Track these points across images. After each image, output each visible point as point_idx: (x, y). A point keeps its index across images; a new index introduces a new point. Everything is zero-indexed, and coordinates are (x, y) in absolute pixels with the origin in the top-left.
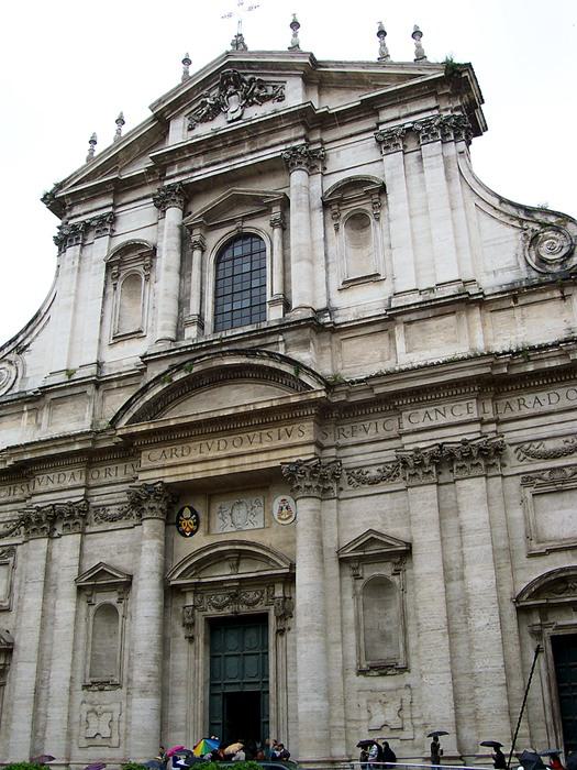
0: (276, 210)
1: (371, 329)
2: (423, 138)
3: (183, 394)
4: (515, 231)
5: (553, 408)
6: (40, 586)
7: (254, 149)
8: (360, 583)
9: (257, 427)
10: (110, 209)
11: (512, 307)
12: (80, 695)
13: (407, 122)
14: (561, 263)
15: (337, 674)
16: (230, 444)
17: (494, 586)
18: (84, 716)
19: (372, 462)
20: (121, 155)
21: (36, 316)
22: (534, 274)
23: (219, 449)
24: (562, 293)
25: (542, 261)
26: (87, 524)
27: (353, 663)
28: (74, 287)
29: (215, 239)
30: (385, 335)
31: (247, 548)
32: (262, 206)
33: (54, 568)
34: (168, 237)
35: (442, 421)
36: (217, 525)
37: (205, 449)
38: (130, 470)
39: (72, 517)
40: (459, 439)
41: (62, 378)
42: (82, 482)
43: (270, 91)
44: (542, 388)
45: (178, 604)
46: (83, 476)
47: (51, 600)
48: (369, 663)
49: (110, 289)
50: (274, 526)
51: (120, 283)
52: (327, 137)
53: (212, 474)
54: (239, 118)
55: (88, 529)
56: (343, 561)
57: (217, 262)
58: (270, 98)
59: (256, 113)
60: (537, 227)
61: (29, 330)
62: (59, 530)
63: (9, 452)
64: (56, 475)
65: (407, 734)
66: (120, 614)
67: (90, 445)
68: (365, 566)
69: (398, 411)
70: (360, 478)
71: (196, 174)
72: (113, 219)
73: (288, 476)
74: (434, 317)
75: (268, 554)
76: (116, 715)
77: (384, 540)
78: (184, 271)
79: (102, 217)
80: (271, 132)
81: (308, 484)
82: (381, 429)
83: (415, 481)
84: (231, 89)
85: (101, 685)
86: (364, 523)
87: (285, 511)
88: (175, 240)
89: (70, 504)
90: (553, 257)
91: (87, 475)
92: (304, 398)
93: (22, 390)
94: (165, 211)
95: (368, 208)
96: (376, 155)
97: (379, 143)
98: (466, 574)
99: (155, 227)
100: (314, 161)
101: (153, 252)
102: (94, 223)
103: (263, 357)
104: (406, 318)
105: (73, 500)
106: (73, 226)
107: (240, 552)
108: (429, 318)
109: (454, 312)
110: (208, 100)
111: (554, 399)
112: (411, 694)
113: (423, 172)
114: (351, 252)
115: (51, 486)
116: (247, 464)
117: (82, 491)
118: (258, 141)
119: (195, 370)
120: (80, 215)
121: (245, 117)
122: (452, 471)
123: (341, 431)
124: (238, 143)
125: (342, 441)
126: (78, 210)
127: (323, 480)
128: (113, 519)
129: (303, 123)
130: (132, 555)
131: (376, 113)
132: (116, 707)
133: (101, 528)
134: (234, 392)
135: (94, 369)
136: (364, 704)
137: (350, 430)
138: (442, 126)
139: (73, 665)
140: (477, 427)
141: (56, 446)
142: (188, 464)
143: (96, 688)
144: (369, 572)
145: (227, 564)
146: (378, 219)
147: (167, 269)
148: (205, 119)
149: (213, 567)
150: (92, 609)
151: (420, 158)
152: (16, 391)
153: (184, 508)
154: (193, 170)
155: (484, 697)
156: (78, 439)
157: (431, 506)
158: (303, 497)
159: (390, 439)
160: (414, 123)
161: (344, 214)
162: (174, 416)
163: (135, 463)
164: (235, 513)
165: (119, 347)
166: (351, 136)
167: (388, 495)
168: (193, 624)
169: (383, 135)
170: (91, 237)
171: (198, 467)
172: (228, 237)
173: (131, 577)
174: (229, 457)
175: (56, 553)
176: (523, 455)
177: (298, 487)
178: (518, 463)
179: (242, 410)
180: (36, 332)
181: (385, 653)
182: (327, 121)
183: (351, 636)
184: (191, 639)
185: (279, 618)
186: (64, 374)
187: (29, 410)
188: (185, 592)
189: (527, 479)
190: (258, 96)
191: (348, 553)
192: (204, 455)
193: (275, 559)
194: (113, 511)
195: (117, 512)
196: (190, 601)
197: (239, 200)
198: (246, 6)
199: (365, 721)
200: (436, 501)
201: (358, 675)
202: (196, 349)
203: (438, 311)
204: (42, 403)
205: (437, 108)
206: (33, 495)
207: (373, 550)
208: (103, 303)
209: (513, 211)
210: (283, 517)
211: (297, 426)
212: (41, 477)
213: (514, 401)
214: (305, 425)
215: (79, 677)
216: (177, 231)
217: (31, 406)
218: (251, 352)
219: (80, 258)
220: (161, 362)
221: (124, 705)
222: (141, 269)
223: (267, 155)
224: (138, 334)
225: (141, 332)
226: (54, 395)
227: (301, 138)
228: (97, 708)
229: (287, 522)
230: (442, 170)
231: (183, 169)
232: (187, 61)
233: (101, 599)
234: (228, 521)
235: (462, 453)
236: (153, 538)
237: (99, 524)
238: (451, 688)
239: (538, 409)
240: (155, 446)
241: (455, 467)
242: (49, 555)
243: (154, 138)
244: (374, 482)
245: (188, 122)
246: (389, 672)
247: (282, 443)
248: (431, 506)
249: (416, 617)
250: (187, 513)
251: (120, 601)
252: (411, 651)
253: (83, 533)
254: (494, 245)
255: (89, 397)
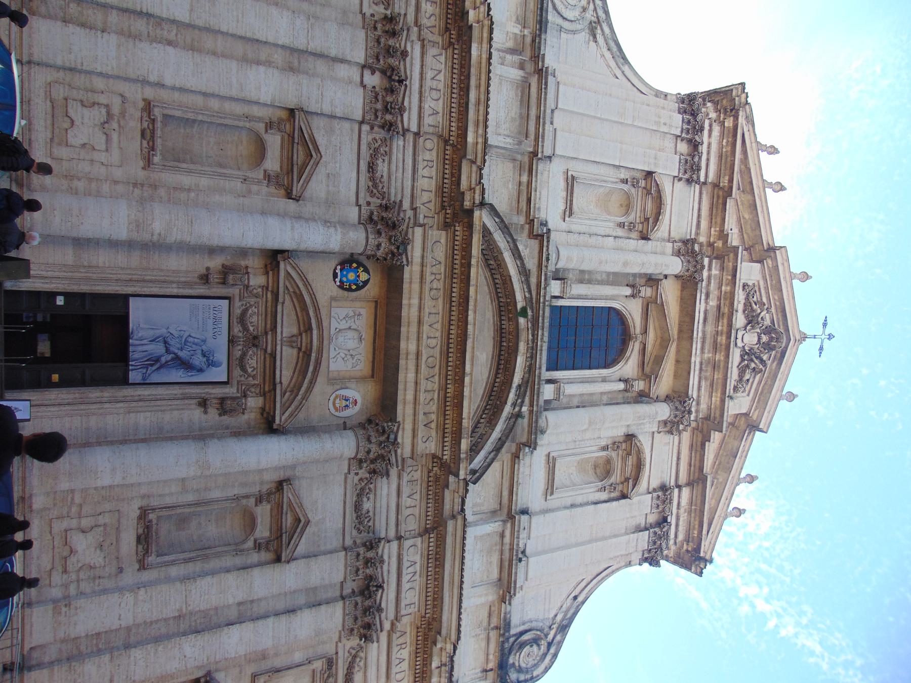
0: (639, 386)
1: (506, 493)
2: (655, 533)
3: (497, 293)
4: (552, 615)
5: (393, 676)
6: (301, 43)
7: (703, 366)
8: (252, 501)
9: (444, 389)
10: (702, 179)
11: (489, 624)
12: (136, 94)
13: (672, 520)
14: (514, 664)
15: (144, 490)
16: (431, 352)
17: (227, 656)
18: (103, 99)
19: (378, 505)
20: (749, 197)
21: (624, 58)
22: (512, 640)
23: (428, 338)
24: (491, 670)
25: (522, 646)
26: (372, 128)
27: (155, 503)
28: (640, 125)
29: (633, 311)
30: (497, 506)
31: (311, 368)
32: (650, 372)
33: (321, 67)
34: (656, 265)
35: (405, 578)
36: (338, 310)
37: (433, 319)
38: (426, 197)
39: (386, 110)
40: (383, 605)
41: (550, 103)
42: (426, 128)
43: (747, 377)
44: (413, 667)
45: (255, 263)
46: (431, 130)
47: (278, 57)
48: (154, 522)
49: (623, 175)
50: (330, 389)
51: (626, 187)
52: (686, 436)
53: (403, 329)
54: (736, 344)
55: (365, 128)
56: (280, 485)
57: (610, 309)
58: (740, 379)
59: (736, 357)
60: (550, 637)
61: (612, 44)
62: (373, 80)
63: (487, 23)
64: (441, 86)
65: (57, 578)
66: (250, 174)
67: (469, 157)
68: (269, 507)
69: (425, 532)
70: (361, 494)
71: (703, 297)
72: (689, 181)
73: (383, 427)
74: (501, 559)
75: (299, 397)
76: (103, 157)
77: (296, 535)
78: (614, 279)
79: (699, 170)
80: (712, 385)
81: (373, 450)
82: (409, 511)
83: (351, 556)
84: (765, 338)
85: (148, 135)
86: (316, 502)
87: (344, 403)
88: (650, 270)
89: (402, 110)
90: (522, 656)
91: (433, 134)
92: (463, 456)
93: (549, 25)
94: (678, 253)
95: (612, 480)
96: (655, 484)
97: (664, 488)
98: (244, 625)
99: (666, 235)
100: (671, 426)
101: (645, 237)
102: (696, 159)
103: (514, 405)
104: (508, 533)
105: (406, 116)
106: (702, 129)
107: (308, 354)
108: (501, 555)
109: (500, 580)
110: (765, 312)
111: (399, 677)
112: (110, 576)
113: (626, 534)
114: (578, 458)
115: (429, 74)
116: (407, 375)
117: (414, 128)
118: (710, 369)
119: (522, 320)
120: (710, 136)
121: (735, 349)
122: (353, 592)
123: (415, 468)
124: (715, 347)
125: (405, 474)
126: (716, 129)
127: (373, 461)
128: (371, 167)
129: (707, 418)
130: (323, 195)
131: (690, 484)
132: (115, 156)
133: (364, 147)
134: (484, 356)
135: (548, 152)
136: (101, 520)
137: (415, 478)
138: (660, 547)
139: (182, 90)
140: (391, 615)
141: (478, 103)
142: (421, 299)
143: (145, 125)
144: (263, 513)
145: (295, 331)
146: (600, 490)
147: (625, 264)
148: (748, 305)
149: (293, 313)
150: (261, 127)
151: (639, 529)
152: (550, 18)
153: (369, 274)
154: (707, 295)
155: (99, 666)
156: (480, 140)
157: (323, 579)
158: (358, 447)
159: (397, 525)
160: (670, 525)
161: (614, 454)
162: (478, 274)
163: (431, 206)
164: (350, 334)
165: (562, 184)
166: (678, 459)
167: (341, 525)
168: (224, 283)
169: (670, 494)
170: (683, 147)
171: (414, 312)
172: (631, 324)
173: (297, 200)
174: (418, 355)
175: (343, 71)
176: (354, 652)
177: (369, 440)
178: (347, 648)
179: (467, 379)
180: (608, 55)
181: (165, 531)
182: (698, 448)
183: (190, 498)
184: (205, 278)
185: (222, 400)
186: (553, 107)
187: (524, 35)
188: (267, 273)
189: (330, 663)
190: (747, 366)
191: (288, 494)
192: (426, 318)
193: (293, 406)
194: (382, 168)
195: (378, 175)
196: (257, 280)
197: (664, 343)
198: (827, 343)
199: (80, 523)
200: (327, 582)
201: (139, 509)
202: (534, 302)
203: (506, 564)
204: (530, 67)
205: (675, 543)
206: (423, 46)
207: (288, 521)
208: (614, 166)
209: (569, 615)
210: (338, 401)
211: (434, 434)
212: (442, 59)
213: (408, 638)
214: (434, 443)
215: (164, 94)
216: (658, 272)
217: (528, 40)
218: (521, 395)
219: (666, 133)
220: (536, 261)
221: (118, 173)
222: (631, 218)
223: (694, 380)
224: (569, 211)
225: (571, 214)
226: (534, 90)
227: (697, 417)
228: (115, 125)
229: (332, 410)
230: (623, 552)
231: (712, 281)
232: (805, 277)
233: (274, 141)
234: (343, 325)
235: (370, 607)
236: (341, 245)
237: (369, 145)
238: (113, 628)
239: (395, 662)
240: (450, 252)
241: (359, 599)
242: (342, 61)
243: (749, 237)
244: (357, 507)
245: (750, 283)
246: (140, 547)
247: (421, 417)
248: (323, 579)
249: (204, 574)
250: (364, 277)
251: (267, 176)
252: (163, 569)
253: (362, 123)
254: (545, 599)
255: (520, 143)
